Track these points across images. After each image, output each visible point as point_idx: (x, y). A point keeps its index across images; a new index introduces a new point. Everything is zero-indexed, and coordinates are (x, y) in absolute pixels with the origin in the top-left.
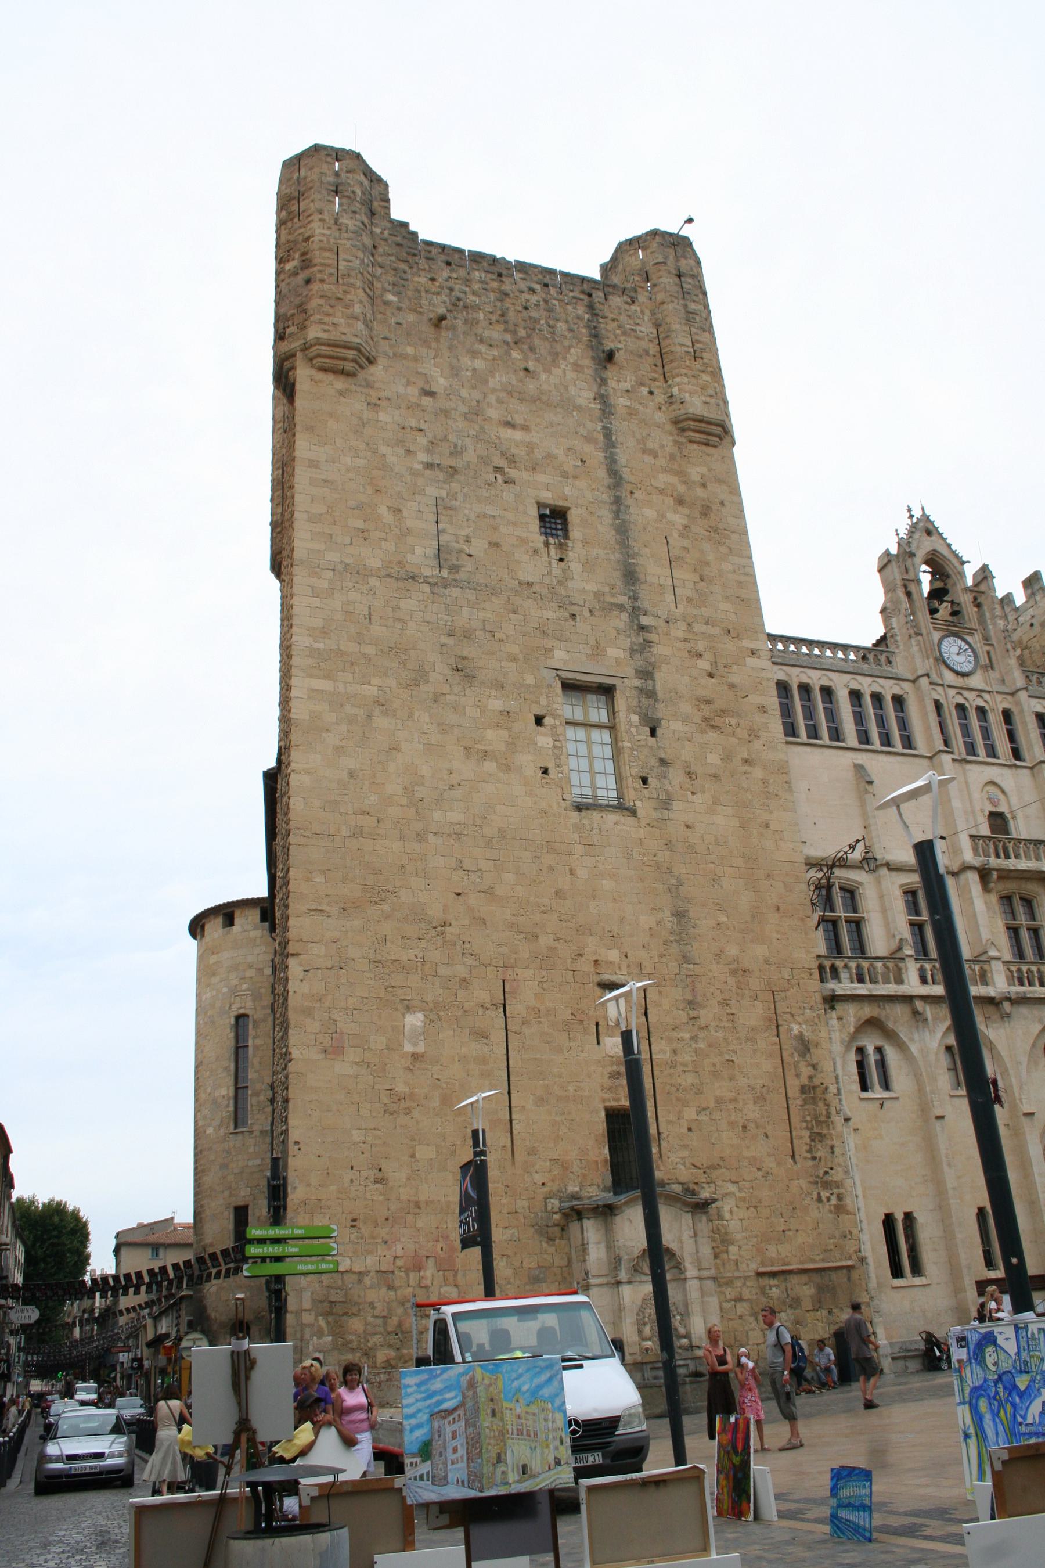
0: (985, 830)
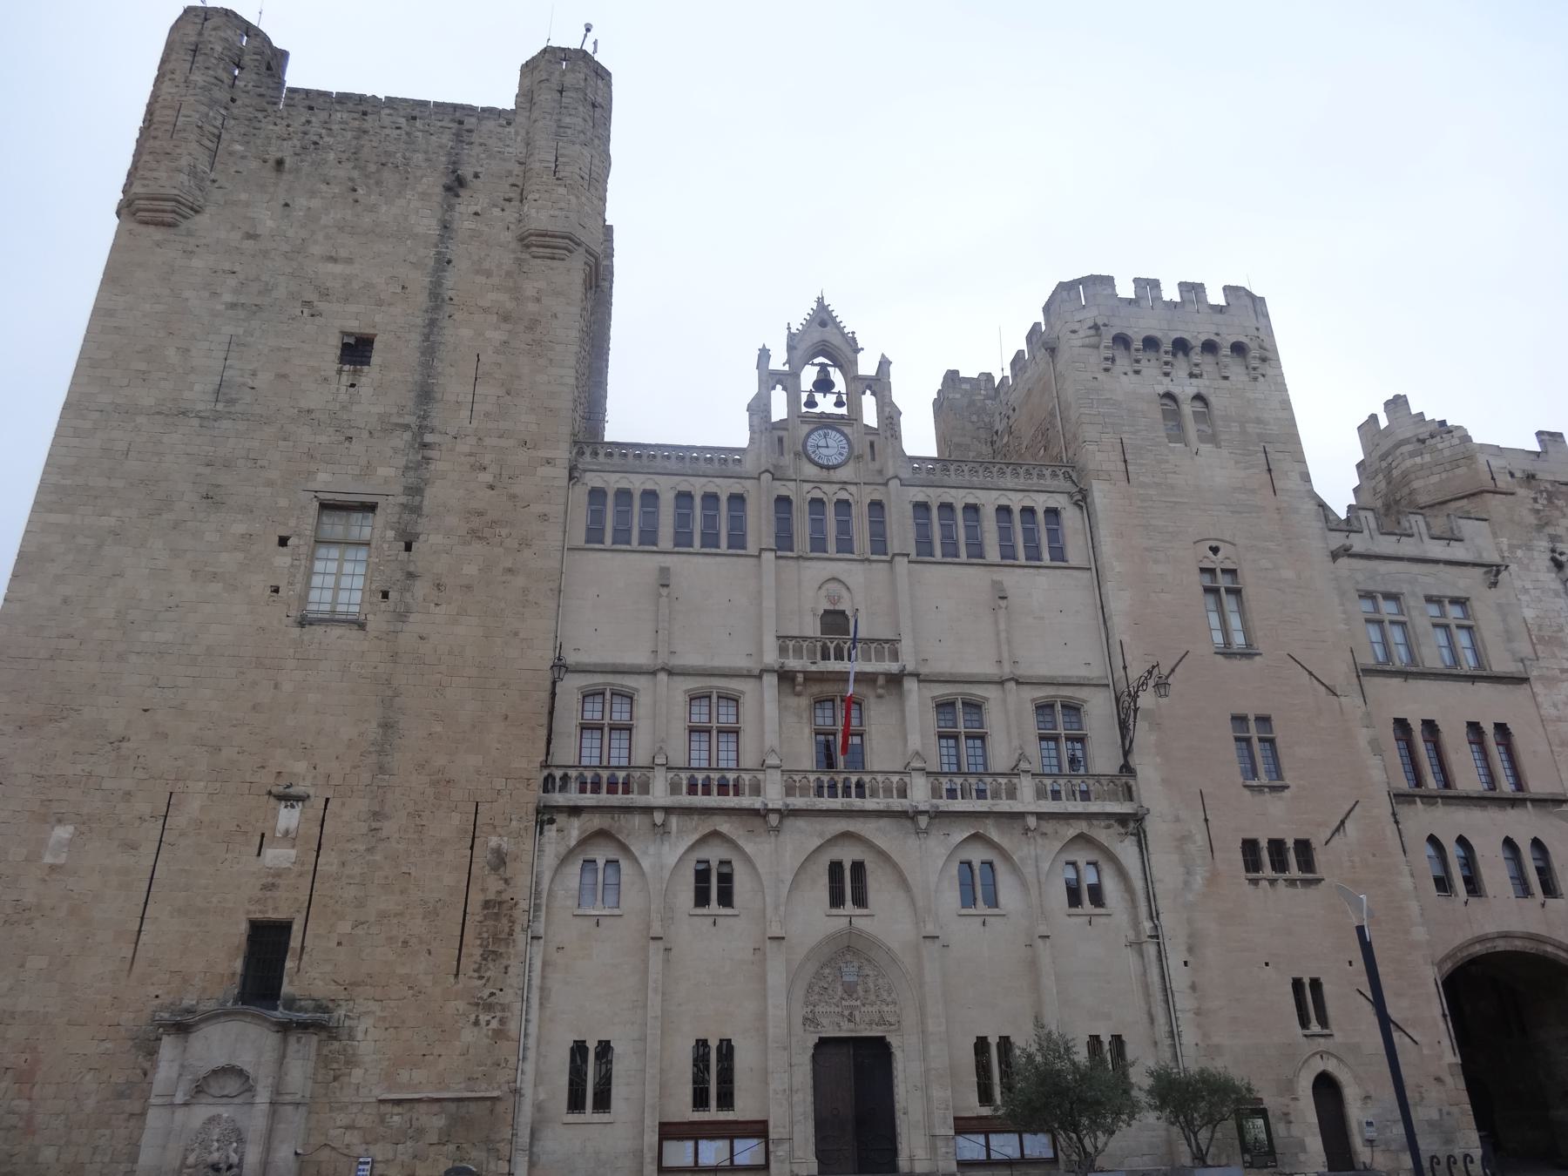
0: (812, 628)
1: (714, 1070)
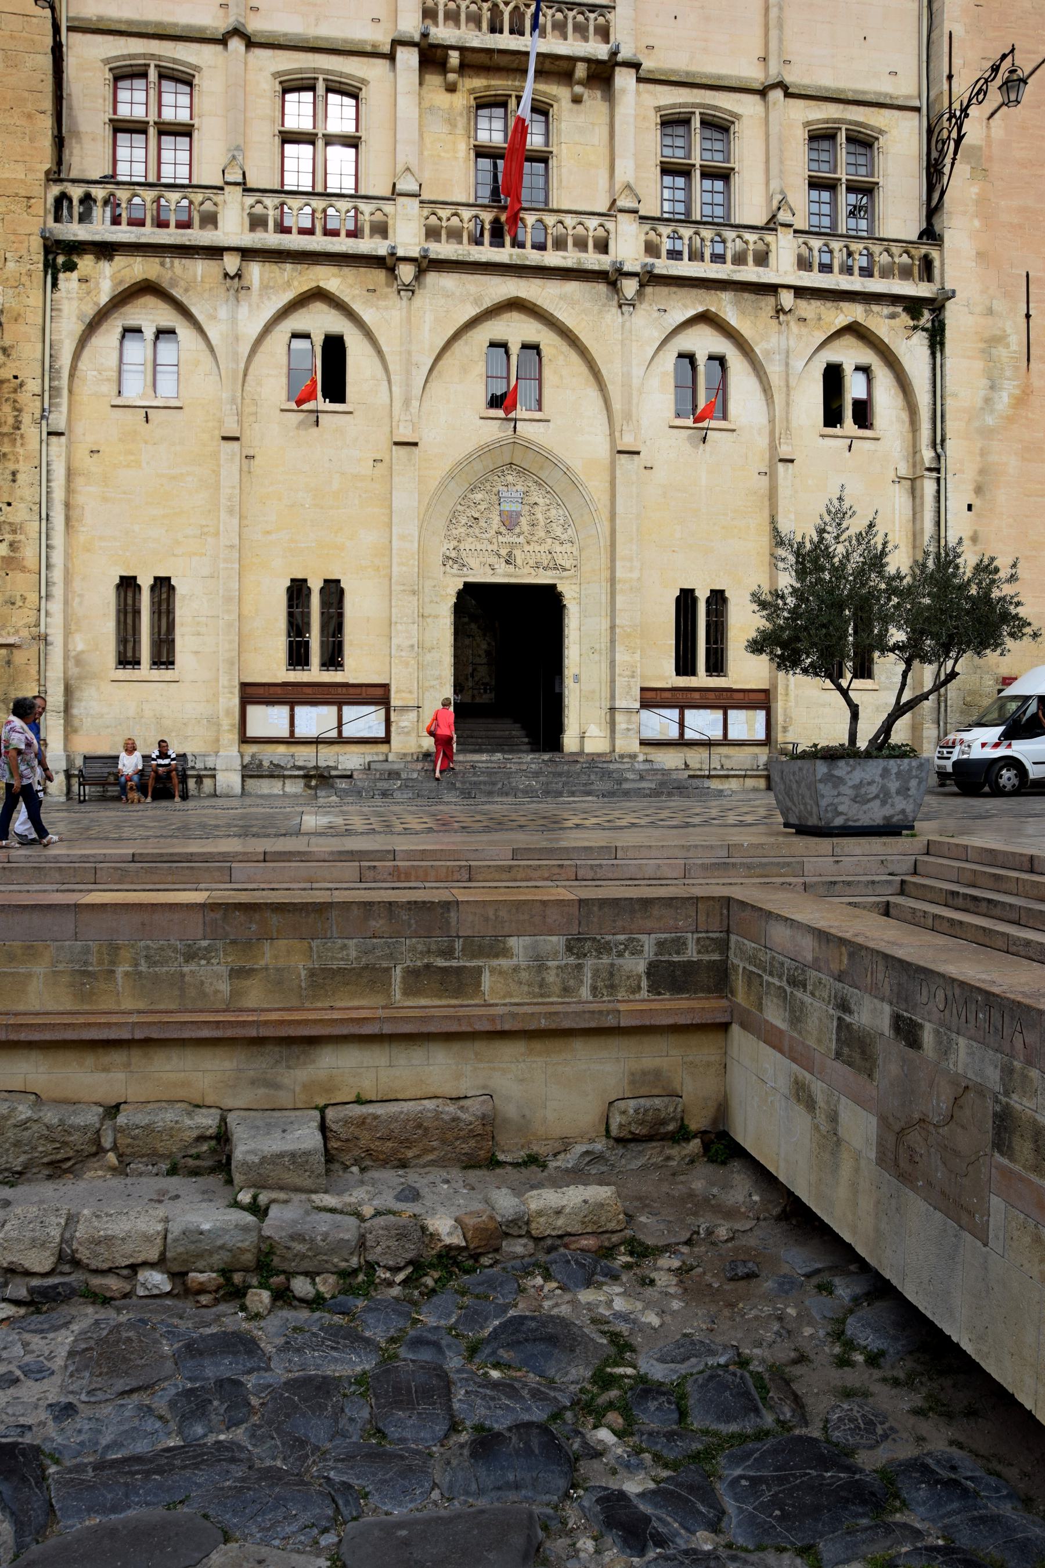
1: (315, 616)
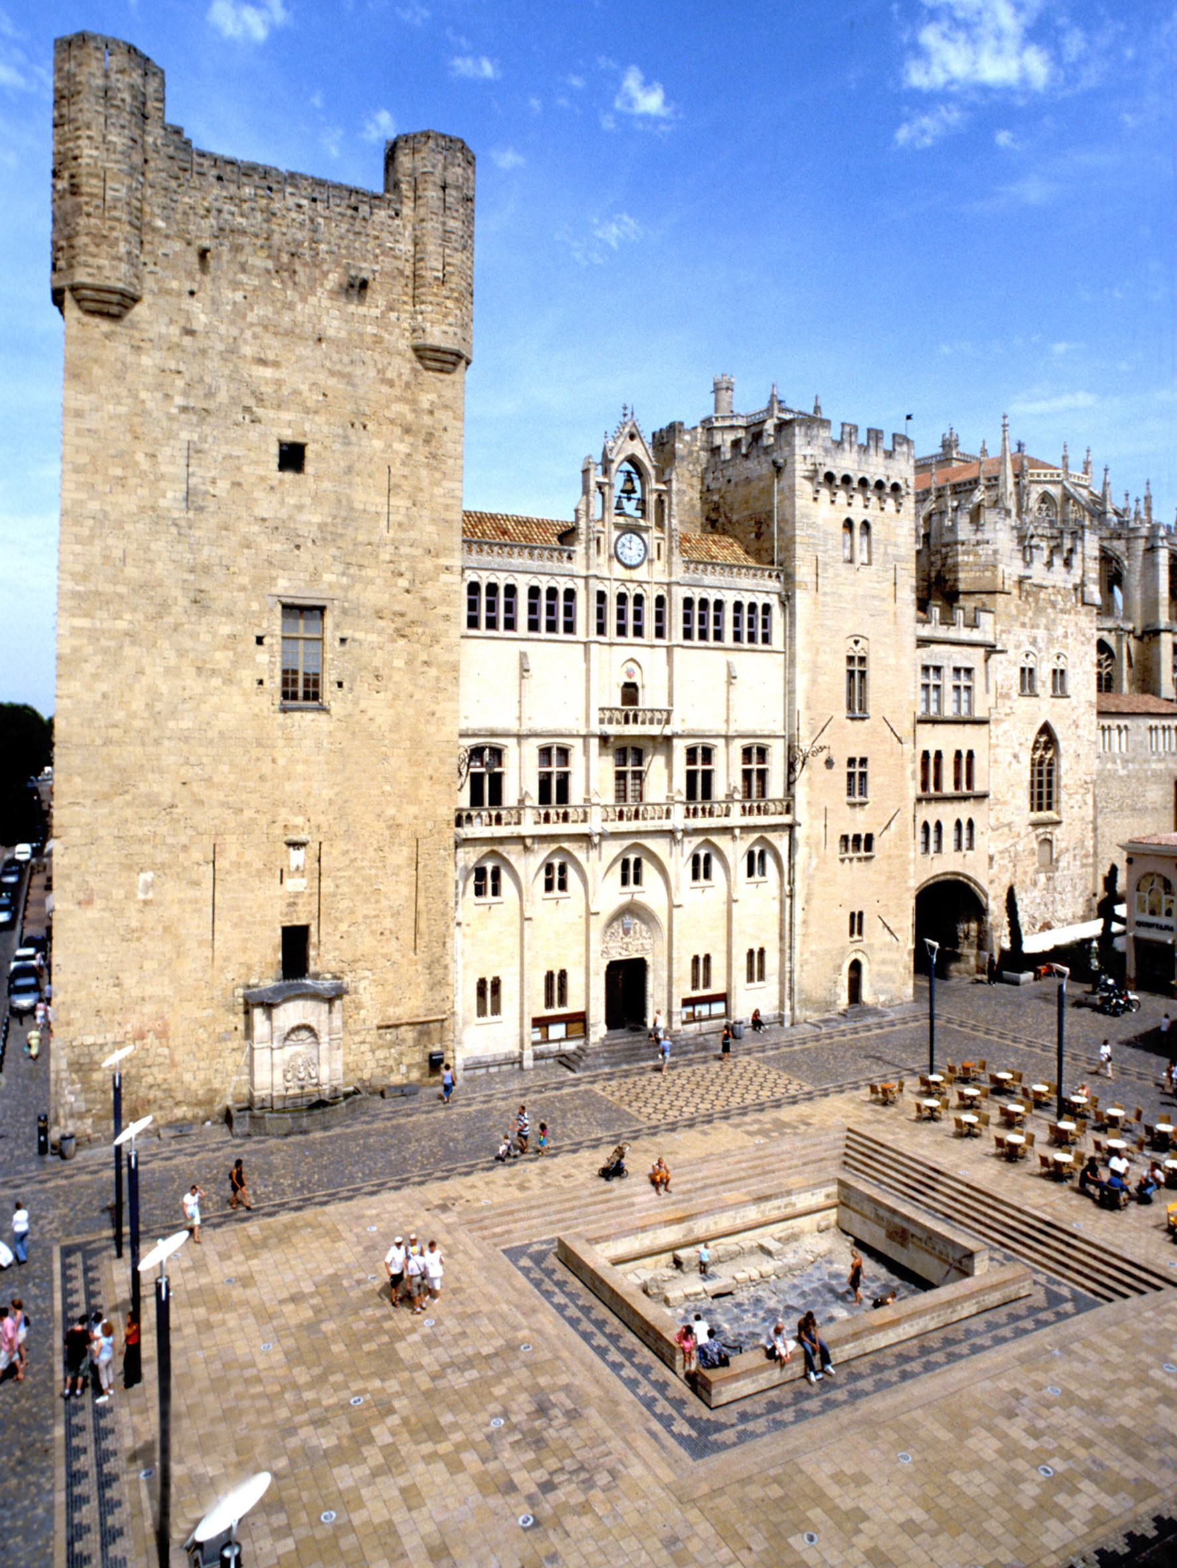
0: (616, 701)
1: (556, 985)
